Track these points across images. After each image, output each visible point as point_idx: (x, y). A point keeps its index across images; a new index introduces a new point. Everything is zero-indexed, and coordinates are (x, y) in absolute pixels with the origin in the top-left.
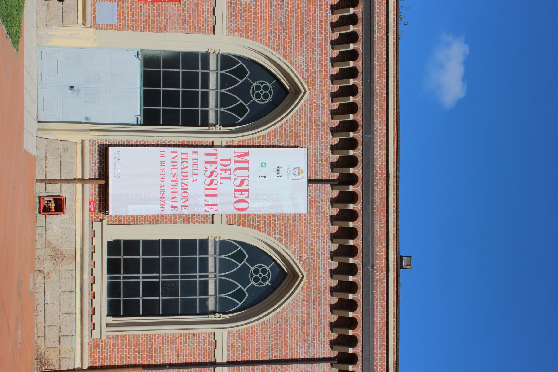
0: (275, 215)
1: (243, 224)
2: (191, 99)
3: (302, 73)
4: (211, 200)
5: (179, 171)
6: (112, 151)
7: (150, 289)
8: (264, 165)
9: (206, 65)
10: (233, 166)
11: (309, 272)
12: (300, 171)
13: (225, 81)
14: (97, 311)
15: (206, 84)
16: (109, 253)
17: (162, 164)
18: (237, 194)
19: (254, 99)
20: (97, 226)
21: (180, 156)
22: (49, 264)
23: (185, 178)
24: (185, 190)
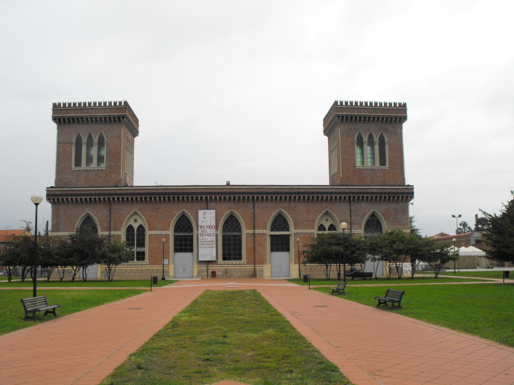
0: (216, 218)
1: (218, 226)
2: (186, 240)
3: (179, 211)
4: (212, 235)
5: (205, 243)
6: (201, 259)
7: (235, 249)
8: (203, 221)
9: (177, 236)
10: (203, 229)
11: (231, 209)
12: (204, 212)
13: (181, 231)
14: (240, 263)
15: (182, 236)
16: (226, 260)
17: (203, 247)
18: (210, 228)
19: (185, 223)
20: (219, 263)
21: (201, 243)
22: (228, 275)
23: (206, 242)
24: (210, 242)
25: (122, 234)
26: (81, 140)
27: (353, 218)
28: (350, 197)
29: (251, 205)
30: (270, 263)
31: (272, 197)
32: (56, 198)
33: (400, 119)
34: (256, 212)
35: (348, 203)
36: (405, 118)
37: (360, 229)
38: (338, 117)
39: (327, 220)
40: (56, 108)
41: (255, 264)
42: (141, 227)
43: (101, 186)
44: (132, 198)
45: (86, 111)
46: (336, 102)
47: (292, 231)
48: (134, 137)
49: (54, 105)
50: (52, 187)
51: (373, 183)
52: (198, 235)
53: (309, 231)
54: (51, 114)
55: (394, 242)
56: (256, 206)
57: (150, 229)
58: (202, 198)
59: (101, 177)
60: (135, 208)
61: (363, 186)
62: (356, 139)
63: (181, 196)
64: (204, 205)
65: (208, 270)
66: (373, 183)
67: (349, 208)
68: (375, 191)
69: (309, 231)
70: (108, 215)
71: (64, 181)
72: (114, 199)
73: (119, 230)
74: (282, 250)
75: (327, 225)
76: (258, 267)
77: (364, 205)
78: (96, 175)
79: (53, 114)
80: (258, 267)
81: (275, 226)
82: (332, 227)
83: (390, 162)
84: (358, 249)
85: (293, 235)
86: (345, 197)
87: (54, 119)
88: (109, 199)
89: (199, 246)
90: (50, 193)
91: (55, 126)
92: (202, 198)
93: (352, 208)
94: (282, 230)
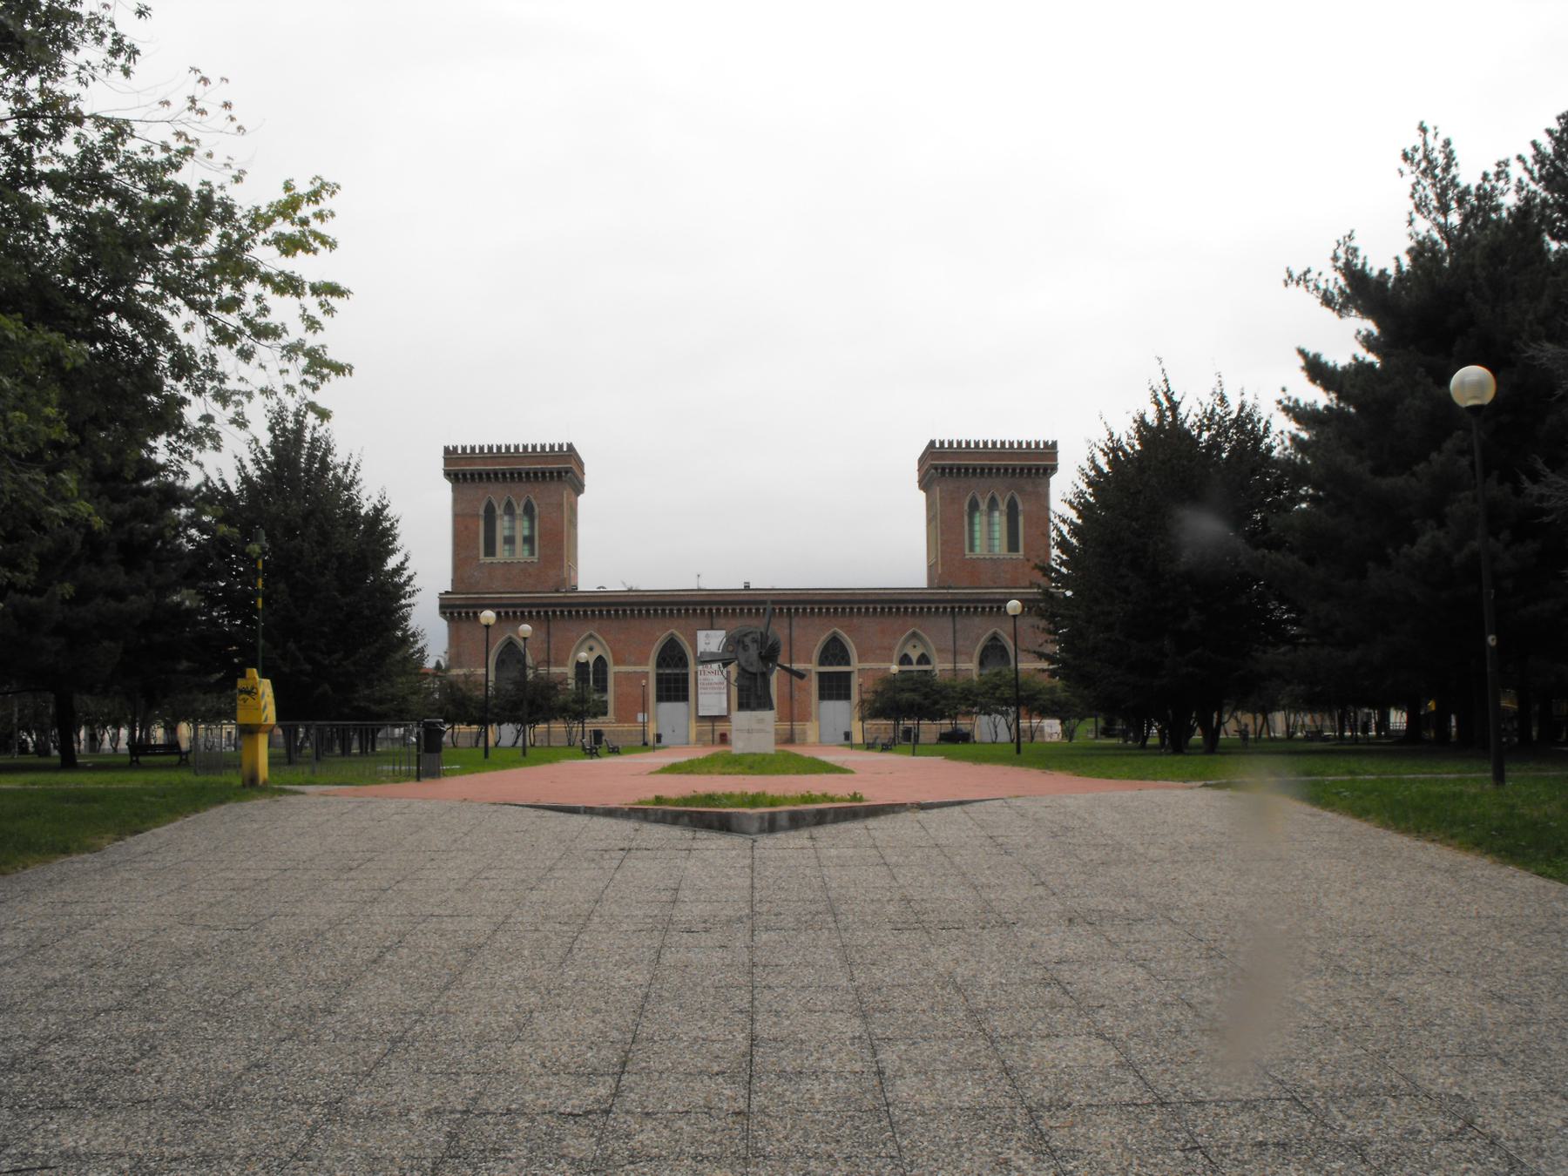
2: (676, 681)
9: (662, 674)
13: (668, 666)
25: (569, 670)
26: (494, 509)
27: (960, 643)
28: (953, 608)
29: (785, 622)
30: (818, 719)
31: (820, 609)
32: (456, 611)
33: (1045, 470)
34: (794, 635)
35: (951, 619)
36: (1054, 469)
37: (971, 662)
38: (936, 469)
39: (915, 647)
40: (450, 454)
41: (792, 721)
42: (600, 658)
44: (585, 612)
45: (501, 460)
46: (932, 443)
47: (855, 665)
48: (578, 495)
49: (447, 450)
50: (447, 593)
51: (995, 583)
52: (696, 673)
53: (883, 665)
54: (442, 466)
55: (1000, 686)
56: (794, 623)
57: (616, 663)
58: (702, 610)
59: (530, 575)
60: (591, 628)
61: (977, 588)
62: (966, 507)
63: (668, 608)
64: (707, 622)
65: (713, 730)
66: (995, 583)
67: (952, 626)
68: (997, 597)
69: (883, 665)
72: (554, 612)
73: (565, 665)
74: (839, 697)
75: (914, 655)
76: (798, 726)
77: (977, 620)
79: (445, 465)
80: (798, 726)
81: (827, 657)
82: (924, 659)
83: (1026, 545)
84: (945, 698)
85: (856, 672)
86: (945, 609)
87: (448, 474)
88: (546, 612)
89: (700, 691)
90: (447, 602)
91: (446, 487)
92: (702, 610)
93: (958, 627)
94: (839, 664)
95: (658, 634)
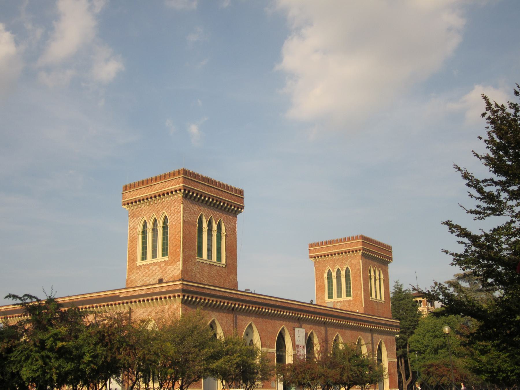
43: (221, 286)
45: (213, 190)
51: (378, 314)
59: (221, 276)
70: (230, 325)
71: (189, 273)
78: (218, 272)
95: (278, 327)
